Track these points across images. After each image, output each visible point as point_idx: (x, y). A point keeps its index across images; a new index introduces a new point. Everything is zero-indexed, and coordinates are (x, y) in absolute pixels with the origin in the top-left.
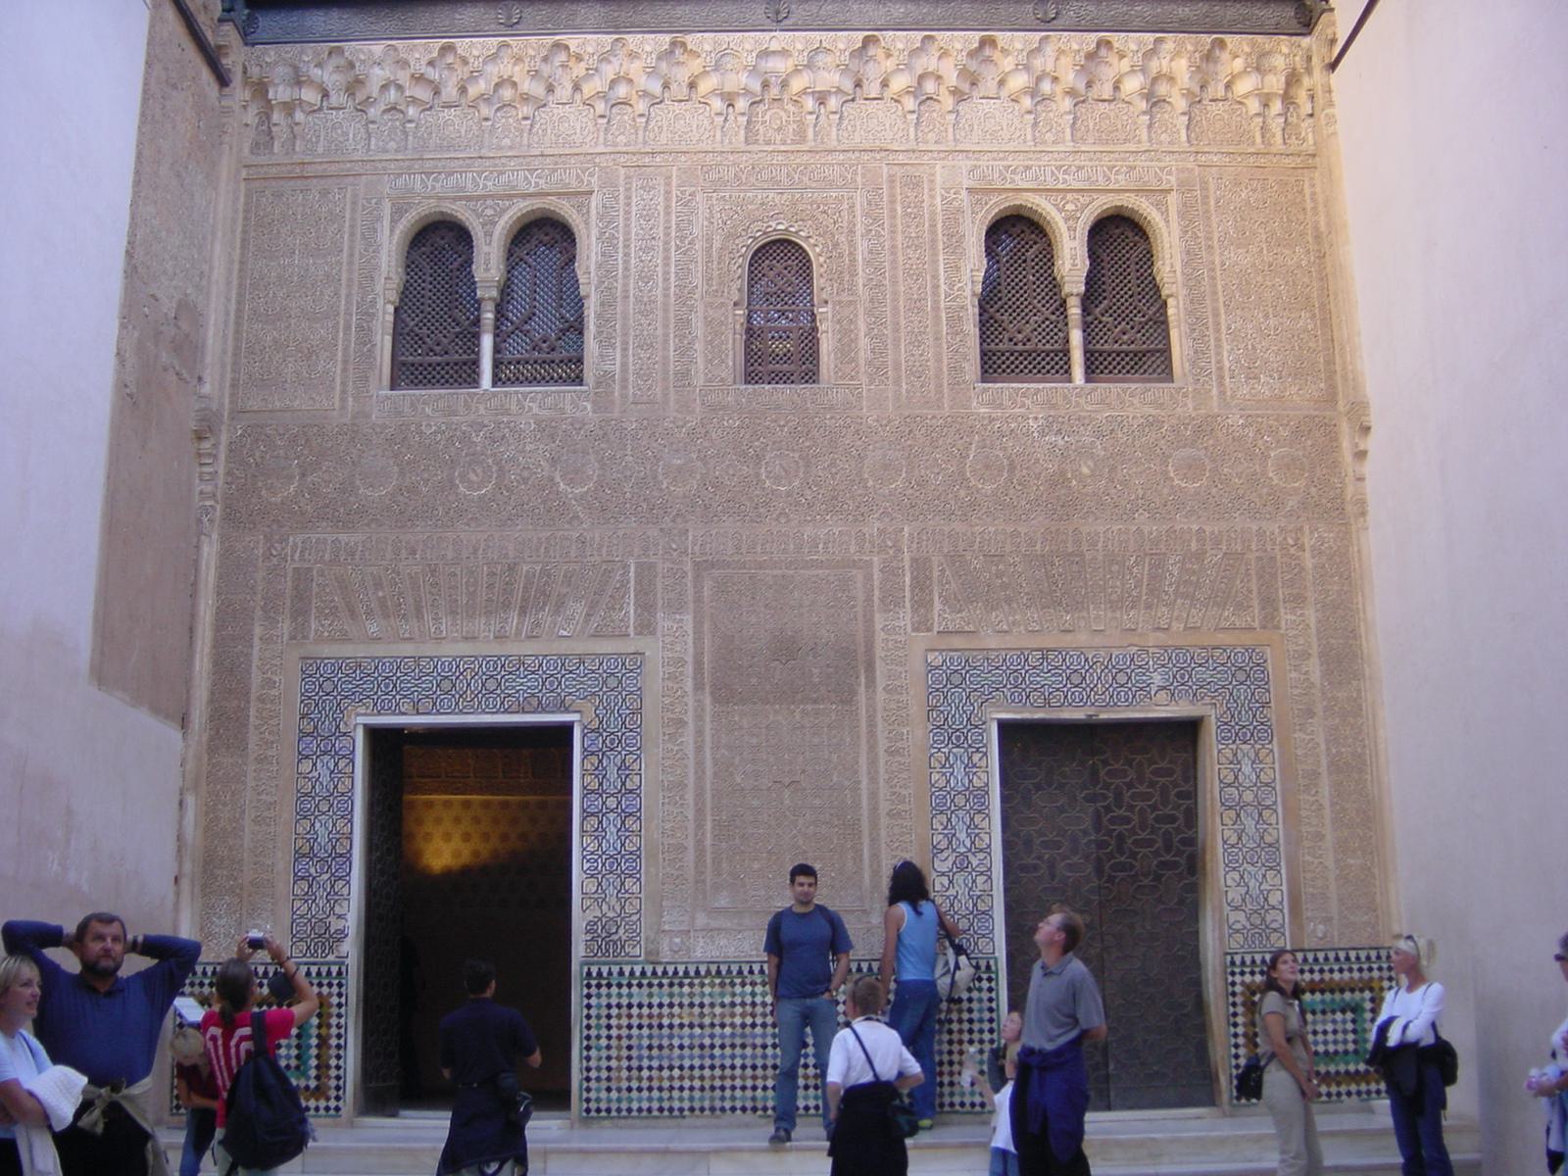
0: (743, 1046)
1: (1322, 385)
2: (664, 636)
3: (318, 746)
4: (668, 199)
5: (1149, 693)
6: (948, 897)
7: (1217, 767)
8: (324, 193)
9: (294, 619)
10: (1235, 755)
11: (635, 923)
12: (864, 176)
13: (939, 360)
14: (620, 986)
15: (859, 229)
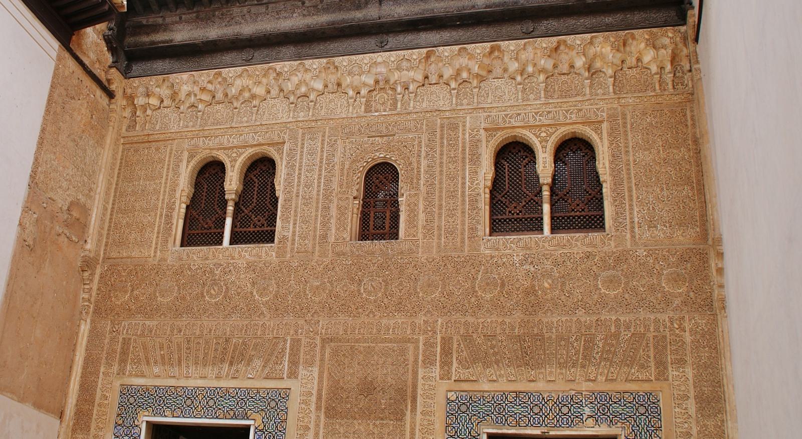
1: (698, 230)
4: (323, 144)
5: (582, 419)
8: (157, 149)
12: (427, 125)
13: (463, 224)
15: (423, 154)
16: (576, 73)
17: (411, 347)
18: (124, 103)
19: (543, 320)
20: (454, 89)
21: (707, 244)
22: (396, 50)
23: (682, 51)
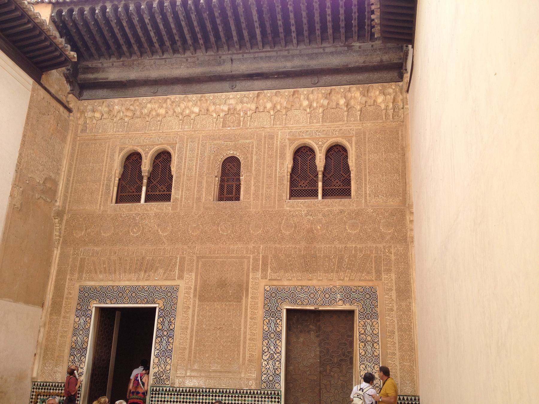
1: (401, 198)
2: (186, 280)
3: (81, 313)
4: (198, 145)
5: (336, 301)
6: (266, 369)
7: (358, 327)
8: (100, 144)
9: (79, 274)
10: (365, 324)
11: (168, 373)
12: (257, 136)
13: (275, 193)
14: (162, 394)
15: (254, 152)
16: (340, 108)
17: (246, 261)
19: (316, 246)
21: (405, 206)
22: (240, 91)
23: (399, 97)
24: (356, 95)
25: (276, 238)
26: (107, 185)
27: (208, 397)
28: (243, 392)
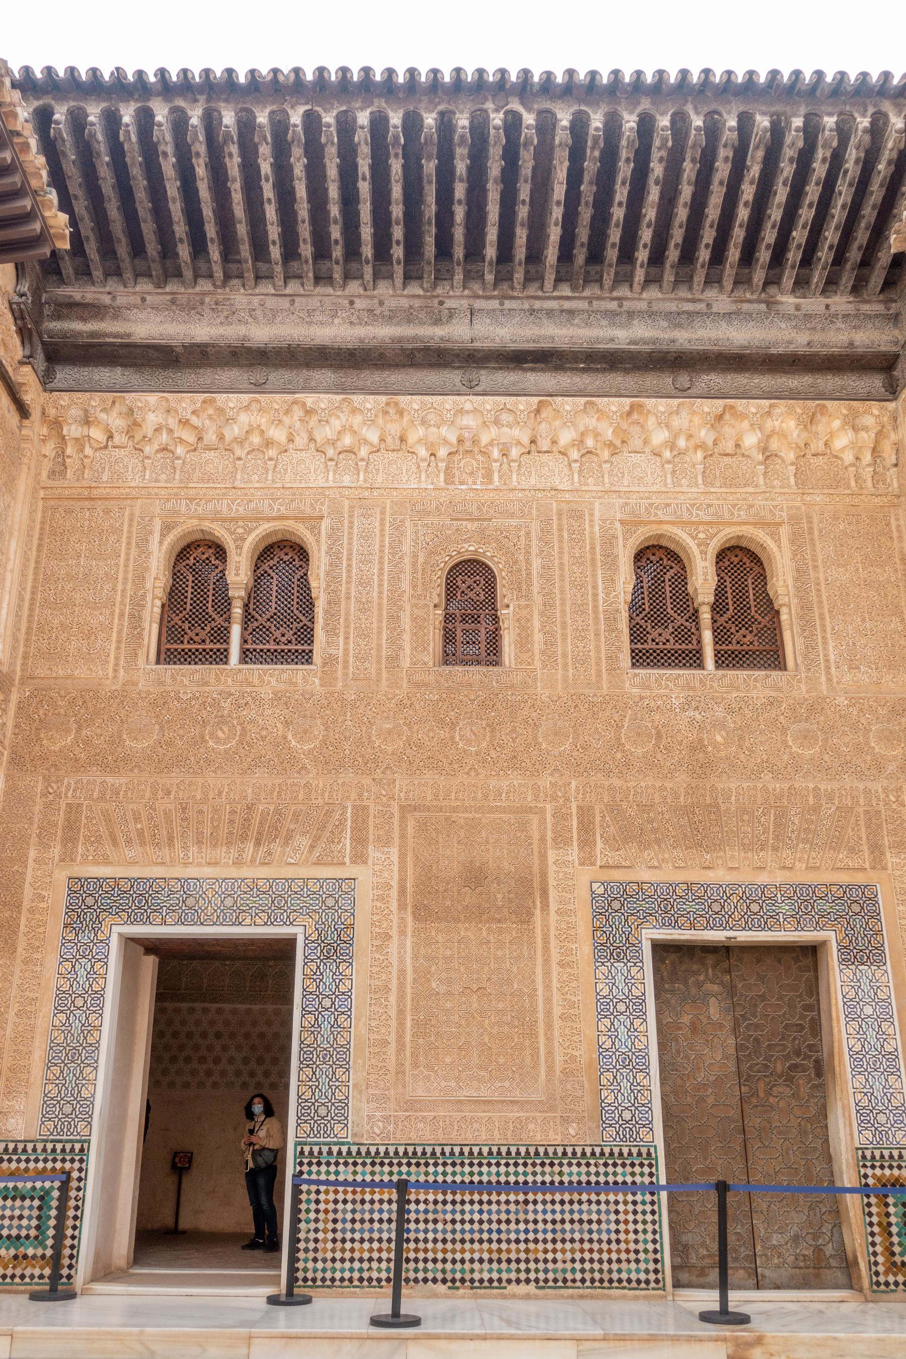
0: (435, 1221)
4: (382, 524)
8: (107, 511)
9: (64, 845)
12: (538, 510)
13: (598, 651)
14: (328, 1164)
15: (534, 550)
16: (743, 455)
18: (45, 431)
20: (576, 461)
24: (784, 425)
25: (611, 762)
26: (132, 616)
27: (458, 1169)
28: (555, 1153)
